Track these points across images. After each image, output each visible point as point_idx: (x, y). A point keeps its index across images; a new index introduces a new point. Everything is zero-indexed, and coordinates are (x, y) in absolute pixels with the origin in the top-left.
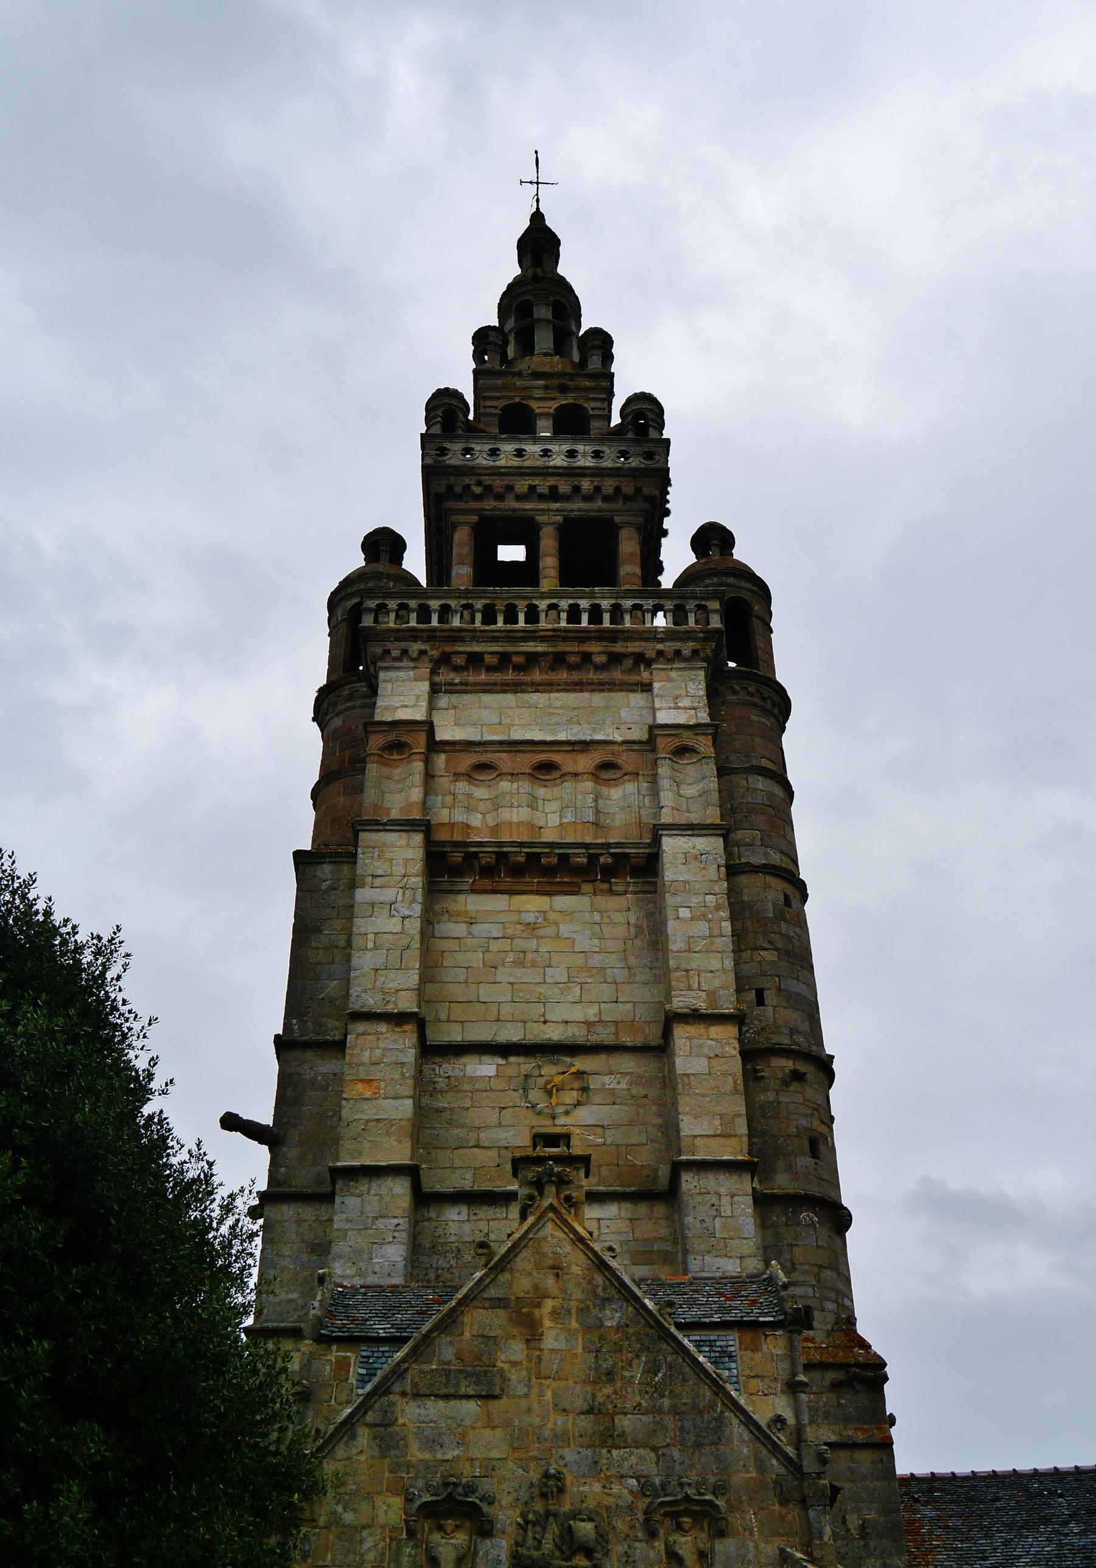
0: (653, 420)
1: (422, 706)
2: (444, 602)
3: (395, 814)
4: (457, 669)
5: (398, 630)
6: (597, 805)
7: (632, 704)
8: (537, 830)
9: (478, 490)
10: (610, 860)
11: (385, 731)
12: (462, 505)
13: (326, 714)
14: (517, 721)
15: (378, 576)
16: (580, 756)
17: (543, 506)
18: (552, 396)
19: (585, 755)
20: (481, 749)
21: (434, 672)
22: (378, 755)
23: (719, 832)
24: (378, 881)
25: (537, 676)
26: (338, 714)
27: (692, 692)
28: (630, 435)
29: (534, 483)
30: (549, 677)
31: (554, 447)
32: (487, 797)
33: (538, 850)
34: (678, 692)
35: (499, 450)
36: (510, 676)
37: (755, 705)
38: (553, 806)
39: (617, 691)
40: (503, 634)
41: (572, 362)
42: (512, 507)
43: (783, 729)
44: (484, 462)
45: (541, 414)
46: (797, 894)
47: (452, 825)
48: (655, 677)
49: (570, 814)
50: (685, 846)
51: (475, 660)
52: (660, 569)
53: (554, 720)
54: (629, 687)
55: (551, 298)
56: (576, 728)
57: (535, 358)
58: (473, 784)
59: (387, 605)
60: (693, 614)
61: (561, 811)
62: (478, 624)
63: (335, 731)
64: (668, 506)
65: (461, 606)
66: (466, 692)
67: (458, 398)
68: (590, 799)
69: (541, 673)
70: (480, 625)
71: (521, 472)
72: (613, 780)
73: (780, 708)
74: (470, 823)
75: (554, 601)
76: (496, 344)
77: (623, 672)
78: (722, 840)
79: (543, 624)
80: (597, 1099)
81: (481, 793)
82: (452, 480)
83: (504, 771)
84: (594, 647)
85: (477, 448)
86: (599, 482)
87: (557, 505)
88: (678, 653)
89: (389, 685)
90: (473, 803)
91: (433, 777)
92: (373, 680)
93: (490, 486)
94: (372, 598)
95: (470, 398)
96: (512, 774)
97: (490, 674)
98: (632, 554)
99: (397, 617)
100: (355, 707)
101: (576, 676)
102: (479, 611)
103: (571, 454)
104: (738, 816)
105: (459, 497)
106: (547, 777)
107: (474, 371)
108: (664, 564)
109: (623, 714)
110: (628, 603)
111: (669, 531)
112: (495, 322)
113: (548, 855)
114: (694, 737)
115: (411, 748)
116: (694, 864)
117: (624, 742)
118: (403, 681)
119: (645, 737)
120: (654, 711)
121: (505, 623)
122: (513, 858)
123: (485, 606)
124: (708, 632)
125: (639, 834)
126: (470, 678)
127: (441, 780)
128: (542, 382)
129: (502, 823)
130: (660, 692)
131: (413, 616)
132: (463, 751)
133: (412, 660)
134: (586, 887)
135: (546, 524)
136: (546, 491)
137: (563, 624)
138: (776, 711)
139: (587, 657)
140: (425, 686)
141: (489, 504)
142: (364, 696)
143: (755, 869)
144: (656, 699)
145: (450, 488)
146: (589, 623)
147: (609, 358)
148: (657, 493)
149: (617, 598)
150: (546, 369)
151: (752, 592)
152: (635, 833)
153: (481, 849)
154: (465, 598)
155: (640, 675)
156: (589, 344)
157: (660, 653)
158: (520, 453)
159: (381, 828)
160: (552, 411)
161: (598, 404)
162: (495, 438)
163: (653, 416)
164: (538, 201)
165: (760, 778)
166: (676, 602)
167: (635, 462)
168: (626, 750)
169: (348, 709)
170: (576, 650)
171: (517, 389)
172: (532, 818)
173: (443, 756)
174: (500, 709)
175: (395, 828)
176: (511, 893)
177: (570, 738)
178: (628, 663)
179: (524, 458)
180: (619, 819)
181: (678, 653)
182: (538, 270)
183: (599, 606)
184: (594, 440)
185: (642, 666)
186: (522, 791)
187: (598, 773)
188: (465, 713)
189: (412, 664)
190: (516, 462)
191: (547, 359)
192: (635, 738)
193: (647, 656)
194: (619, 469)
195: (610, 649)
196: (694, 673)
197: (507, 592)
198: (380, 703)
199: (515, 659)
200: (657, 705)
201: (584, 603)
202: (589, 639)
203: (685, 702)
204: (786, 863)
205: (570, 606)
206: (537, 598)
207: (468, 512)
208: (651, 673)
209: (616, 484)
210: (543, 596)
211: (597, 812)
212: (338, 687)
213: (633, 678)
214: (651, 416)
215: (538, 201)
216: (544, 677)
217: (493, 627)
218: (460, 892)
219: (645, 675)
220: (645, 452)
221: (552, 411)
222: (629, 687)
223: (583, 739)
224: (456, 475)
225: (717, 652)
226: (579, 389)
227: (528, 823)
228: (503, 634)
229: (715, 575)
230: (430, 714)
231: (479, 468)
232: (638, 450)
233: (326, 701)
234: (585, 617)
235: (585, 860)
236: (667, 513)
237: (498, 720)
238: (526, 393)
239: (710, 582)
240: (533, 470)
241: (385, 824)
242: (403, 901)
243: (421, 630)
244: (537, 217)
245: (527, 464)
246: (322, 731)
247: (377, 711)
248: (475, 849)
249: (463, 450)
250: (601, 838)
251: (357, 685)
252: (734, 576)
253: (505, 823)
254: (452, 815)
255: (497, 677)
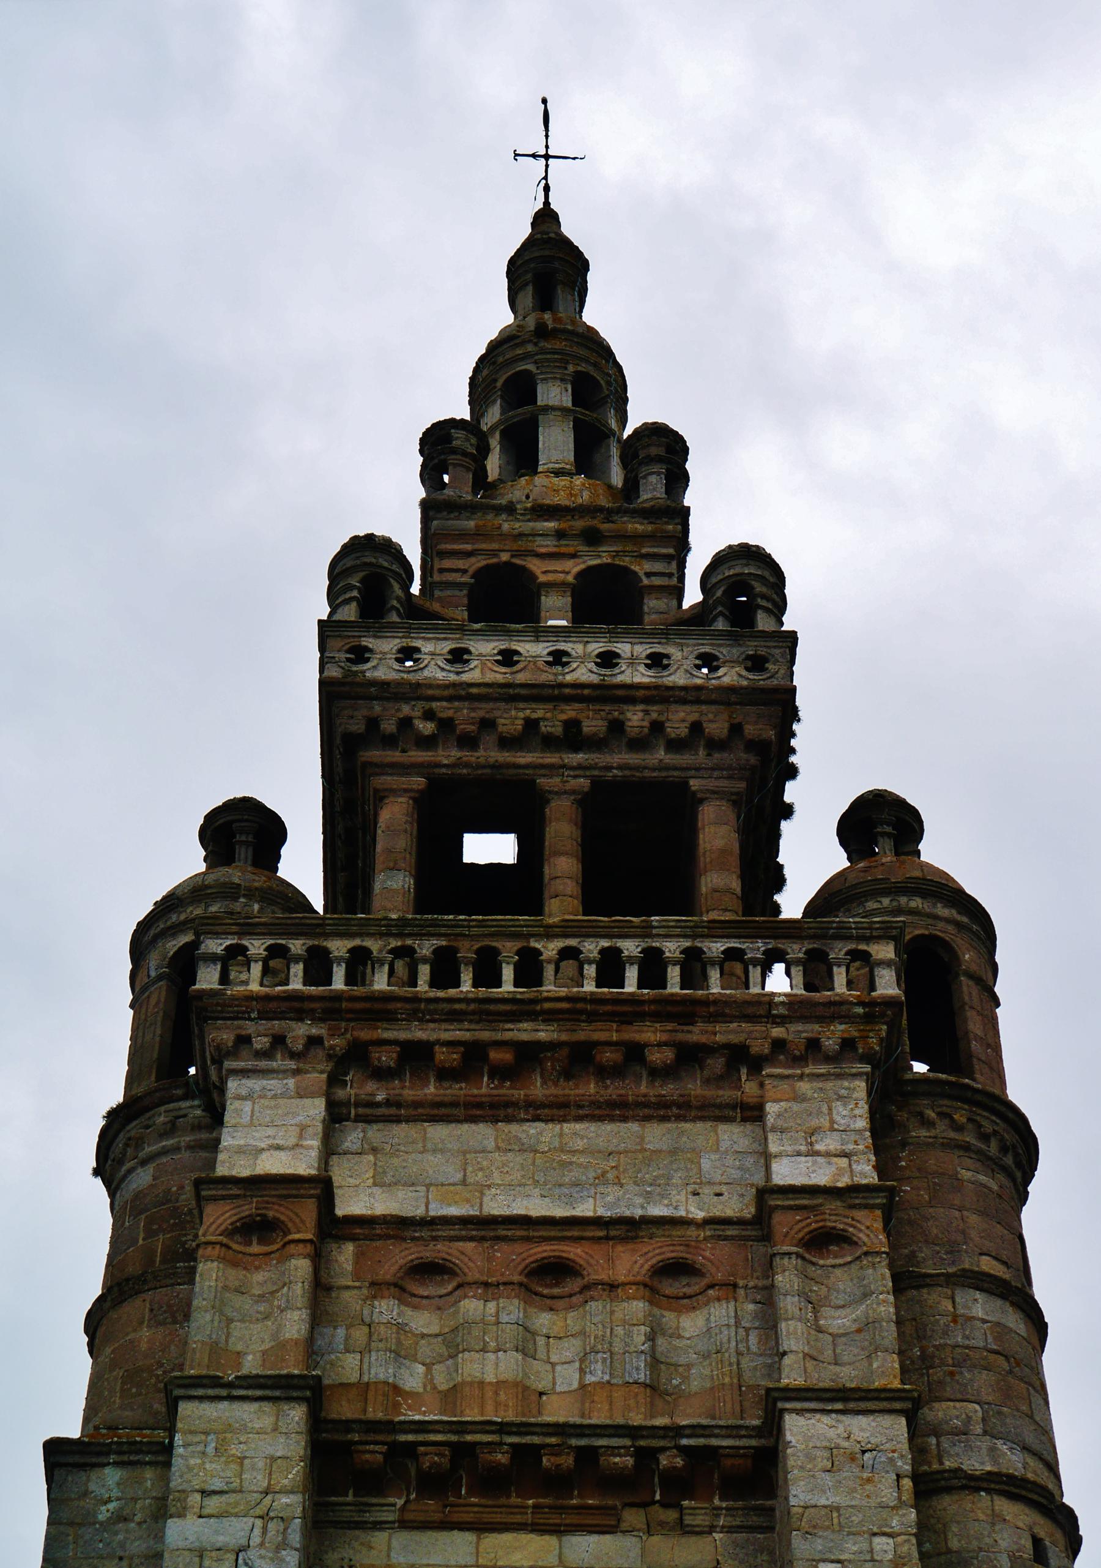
0: (764, 597)
1: (311, 1147)
2: (357, 942)
3: (251, 1365)
4: (381, 1074)
5: (267, 998)
6: (653, 1348)
7: (724, 1146)
8: (534, 1397)
9: (427, 728)
10: (679, 1462)
11: (237, 1197)
12: (394, 756)
13: (120, 1162)
14: (497, 1178)
15: (230, 892)
16: (620, 1248)
17: (551, 759)
18: (571, 550)
19: (630, 1246)
20: (425, 1233)
21: (335, 1080)
22: (222, 1245)
23: (897, 1405)
24: (213, 1504)
25: (538, 1089)
26: (144, 1163)
27: (841, 1121)
28: (720, 625)
29: (534, 716)
30: (561, 1092)
31: (574, 648)
32: (434, 1329)
33: (536, 1440)
34: (814, 1122)
35: (467, 651)
36: (485, 1088)
37: (966, 1148)
38: (569, 1349)
39: (694, 1119)
40: (472, 1006)
41: (610, 487)
42: (492, 760)
43: (1024, 1197)
44: (440, 675)
45: (550, 585)
46: (1059, 1535)
47: (364, 1389)
48: (770, 1093)
49: (599, 1366)
50: (831, 1433)
52: (778, 881)
53: (573, 1175)
54: (717, 1112)
55: (571, 368)
56: (612, 1193)
57: (539, 480)
58: (407, 1305)
59: (246, 949)
60: (843, 969)
61: (582, 1361)
62: (422, 985)
63: (138, 1195)
64: (793, 759)
65: (390, 952)
66: (397, 1120)
67: (390, 554)
68: (639, 1335)
69: (544, 1083)
70: (426, 988)
71: (509, 694)
72: (685, 1297)
73: (1016, 1155)
74: (400, 1383)
75: (572, 942)
76: (465, 454)
77: (707, 1082)
78: (903, 1421)
79: (549, 988)
81: (423, 1321)
82: (377, 708)
83: (469, 1278)
84: (649, 1033)
85: (427, 647)
86: (660, 713)
87: (579, 757)
88: (813, 1044)
89: (247, 1106)
90: (408, 1342)
91: (329, 1289)
92: (215, 1095)
93: (451, 720)
94: (217, 935)
95: (414, 554)
96: (486, 1285)
97: (446, 1084)
98: (723, 852)
99: (266, 971)
100: (177, 1149)
101: (613, 1090)
102: (425, 960)
103: (608, 660)
104: (937, 1374)
105: (390, 741)
106: (556, 1291)
107: (425, 505)
108: (786, 871)
109: (706, 1164)
110: (716, 947)
111: (796, 808)
112: (463, 412)
113: (556, 1451)
114: (847, 1212)
115: (287, 1232)
116: (849, 1472)
117: (708, 1222)
118: (275, 1097)
119: (749, 1212)
120: (767, 1158)
121: (475, 985)
122: (485, 1457)
123: (438, 951)
124: (874, 1003)
125: (738, 1409)
126: (406, 1092)
127: (346, 1295)
128: (551, 525)
129: (463, 1383)
130: (780, 1123)
131: (297, 970)
132: (388, 1237)
133: (293, 1055)
134: (633, 1517)
135: (556, 793)
136: (558, 730)
137: (589, 987)
138: (1009, 1160)
139: (635, 1053)
140: (316, 1109)
141: (447, 755)
142: (197, 1127)
143: (974, 1483)
144: (770, 1136)
145: (373, 723)
146: (640, 986)
147: (679, 479)
148: (771, 734)
149: (694, 937)
150: (561, 499)
151: (958, 925)
152: (729, 1406)
153: (420, 1438)
154: (400, 935)
155: (739, 1087)
156: (642, 455)
157: (779, 1045)
158: (508, 658)
159: (224, 1392)
160: (570, 579)
161: (658, 567)
162: (461, 629)
163: (764, 590)
164: (547, 189)
165: (978, 1295)
166: (808, 945)
167: (729, 676)
168: (712, 1237)
169: (165, 1152)
170: (615, 1037)
171: (503, 537)
172: (525, 1374)
173: (349, 1248)
174: (464, 1153)
175: (250, 1393)
176: (481, 1528)
177: (601, 1212)
178: (716, 1064)
179: (515, 668)
180: (699, 1378)
181: (813, 1044)
182: (547, 316)
183: (659, 952)
184: (652, 634)
185: (744, 1071)
186: (504, 1318)
187: (655, 1283)
188: (395, 1161)
189: (292, 1064)
190: (499, 675)
191: (562, 482)
192: (729, 1213)
193: (754, 1050)
194: (698, 688)
195: (680, 1037)
196: (846, 1084)
197: (481, 924)
198: (228, 1140)
199: (494, 1055)
200: (773, 1148)
201: (630, 947)
202: (641, 1016)
203: (828, 1143)
204: (1034, 1471)
205: (603, 951)
206: (538, 936)
208: (762, 1085)
209: (694, 717)
210: (549, 933)
211: (655, 1362)
212: (148, 1109)
213: (726, 1094)
214: (759, 588)
215: (547, 189)
216: (553, 1091)
217: (452, 992)
218: (378, 1526)
219: (750, 1088)
220: (748, 658)
221: (570, 579)
222: (717, 1112)
223: (628, 1213)
224: (388, 699)
225: (890, 1044)
226: (622, 537)
227: (516, 1384)
228: (472, 1006)
229: (886, 892)
230: (327, 1163)
231: (430, 686)
232: (736, 652)
233: (121, 1135)
234: (632, 975)
235: (630, 1461)
236: (792, 772)
237: (459, 1176)
238: (521, 544)
239: (876, 906)
240: (535, 691)
241: (230, 1385)
242: (262, 1544)
243: (311, 998)
244: (546, 218)
245: (521, 678)
246: (112, 1194)
247: (221, 1157)
248: (410, 1437)
249: (400, 651)
250: (662, 1415)
251: (184, 1104)
252: (924, 894)
253: (471, 1384)
254: (365, 1366)
255: (458, 1090)
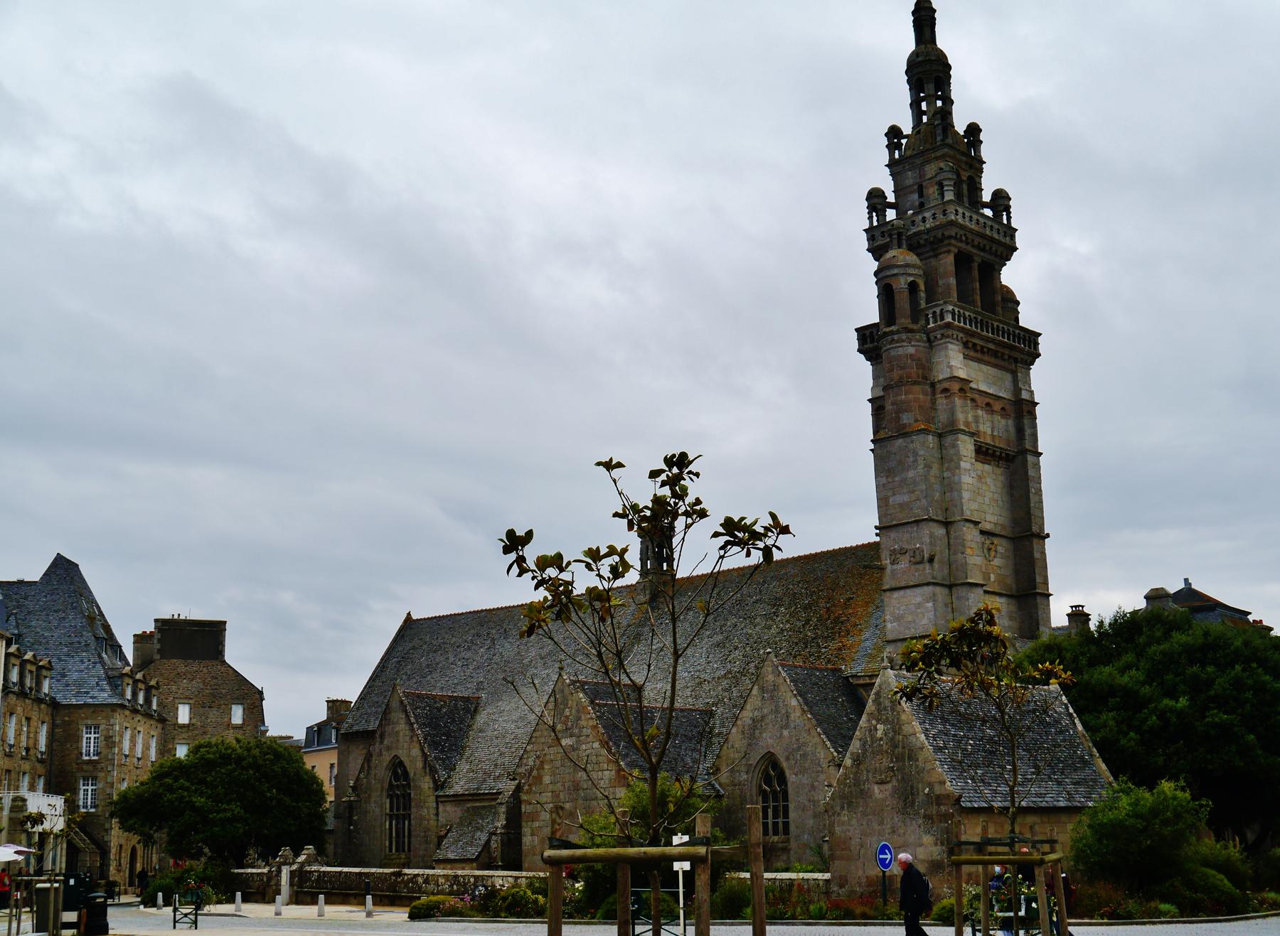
9: (964, 238)
25: (986, 358)
51: (975, 345)
80: (998, 555)
84: (1007, 352)
87: (982, 254)
88: (1026, 360)
134: (992, 463)
139: (1003, 354)
141: (963, 245)
207: (956, 246)
